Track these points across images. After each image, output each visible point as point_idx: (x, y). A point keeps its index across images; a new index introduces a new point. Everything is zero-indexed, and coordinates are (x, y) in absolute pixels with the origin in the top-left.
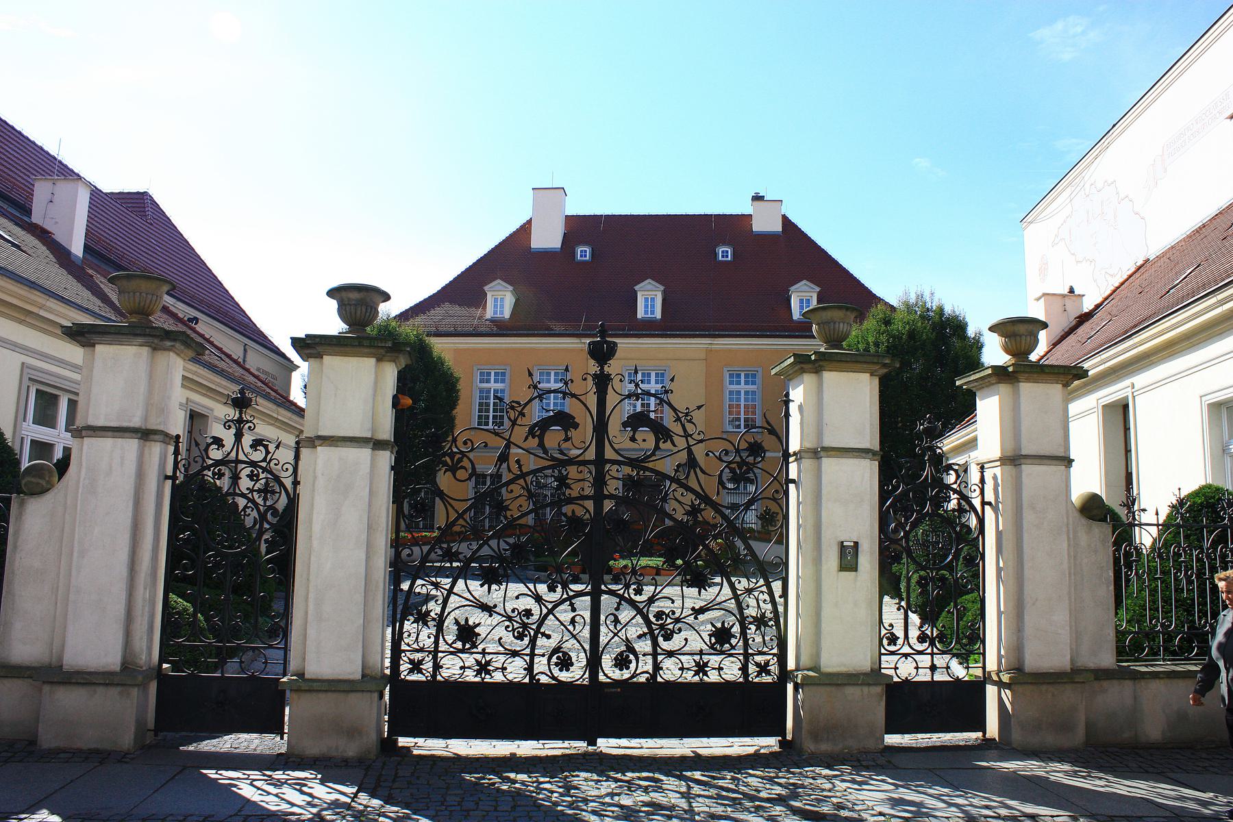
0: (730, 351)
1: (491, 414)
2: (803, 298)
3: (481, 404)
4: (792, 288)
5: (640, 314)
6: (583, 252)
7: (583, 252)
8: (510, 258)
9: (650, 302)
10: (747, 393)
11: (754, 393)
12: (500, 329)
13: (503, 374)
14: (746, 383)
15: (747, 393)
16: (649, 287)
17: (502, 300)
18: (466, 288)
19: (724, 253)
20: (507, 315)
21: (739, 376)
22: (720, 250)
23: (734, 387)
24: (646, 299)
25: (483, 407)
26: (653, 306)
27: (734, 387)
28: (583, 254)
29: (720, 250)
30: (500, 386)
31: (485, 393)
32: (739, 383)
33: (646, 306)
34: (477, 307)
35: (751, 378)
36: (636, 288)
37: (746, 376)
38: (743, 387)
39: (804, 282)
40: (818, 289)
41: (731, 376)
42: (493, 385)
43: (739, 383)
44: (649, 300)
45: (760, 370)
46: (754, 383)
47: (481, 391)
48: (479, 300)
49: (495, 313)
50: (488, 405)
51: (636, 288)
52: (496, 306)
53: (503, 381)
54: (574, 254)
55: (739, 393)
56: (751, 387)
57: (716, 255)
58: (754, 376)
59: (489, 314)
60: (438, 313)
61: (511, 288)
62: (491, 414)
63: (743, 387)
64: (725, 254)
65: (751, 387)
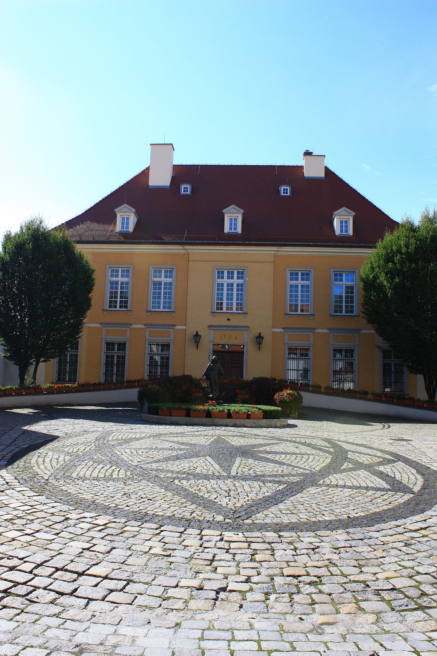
0: (291, 256)
1: (119, 300)
2: (342, 222)
3: (111, 293)
4: (335, 213)
5: (227, 229)
6: (186, 189)
7: (186, 189)
8: (135, 191)
9: (233, 221)
10: (302, 286)
11: (308, 286)
12: (126, 238)
13: (128, 271)
14: (302, 279)
15: (302, 286)
16: (233, 211)
17: (128, 219)
18: (103, 211)
19: (285, 190)
20: (131, 229)
21: (297, 274)
22: (282, 188)
23: (294, 282)
24: (231, 220)
25: (113, 295)
26: (235, 224)
27: (294, 282)
28: (186, 189)
29: (282, 188)
30: (125, 279)
31: (114, 284)
32: (297, 279)
33: (231, 224)
34: (110, 224)
35: (306, 276)
36: (224, 211)
37: (302, 274)
38: (300, 282)
39: (344, 208)
40: (354, 214)
41: (291, 274)
42: (120, 279)
43: (297, 279)
44: (233, 219)
45: (312, 270)
46: (308, 279)
47: (112, 283)
48: (112, 220)
49: (123, 227)
50: (116, 293)
51: (224, 211)
52: (123, 223)
53: (127, 276)
54: (179, 190)
55: (297, 286)
56: (305, 283)
57: (279, 192)
58: (308, 274)
59: (118, 228)
60: (81, 228)
61: (134, 210)
62: (119, 300)
63: (300, 282)
64: (285, 191)
65: (305, 283)
